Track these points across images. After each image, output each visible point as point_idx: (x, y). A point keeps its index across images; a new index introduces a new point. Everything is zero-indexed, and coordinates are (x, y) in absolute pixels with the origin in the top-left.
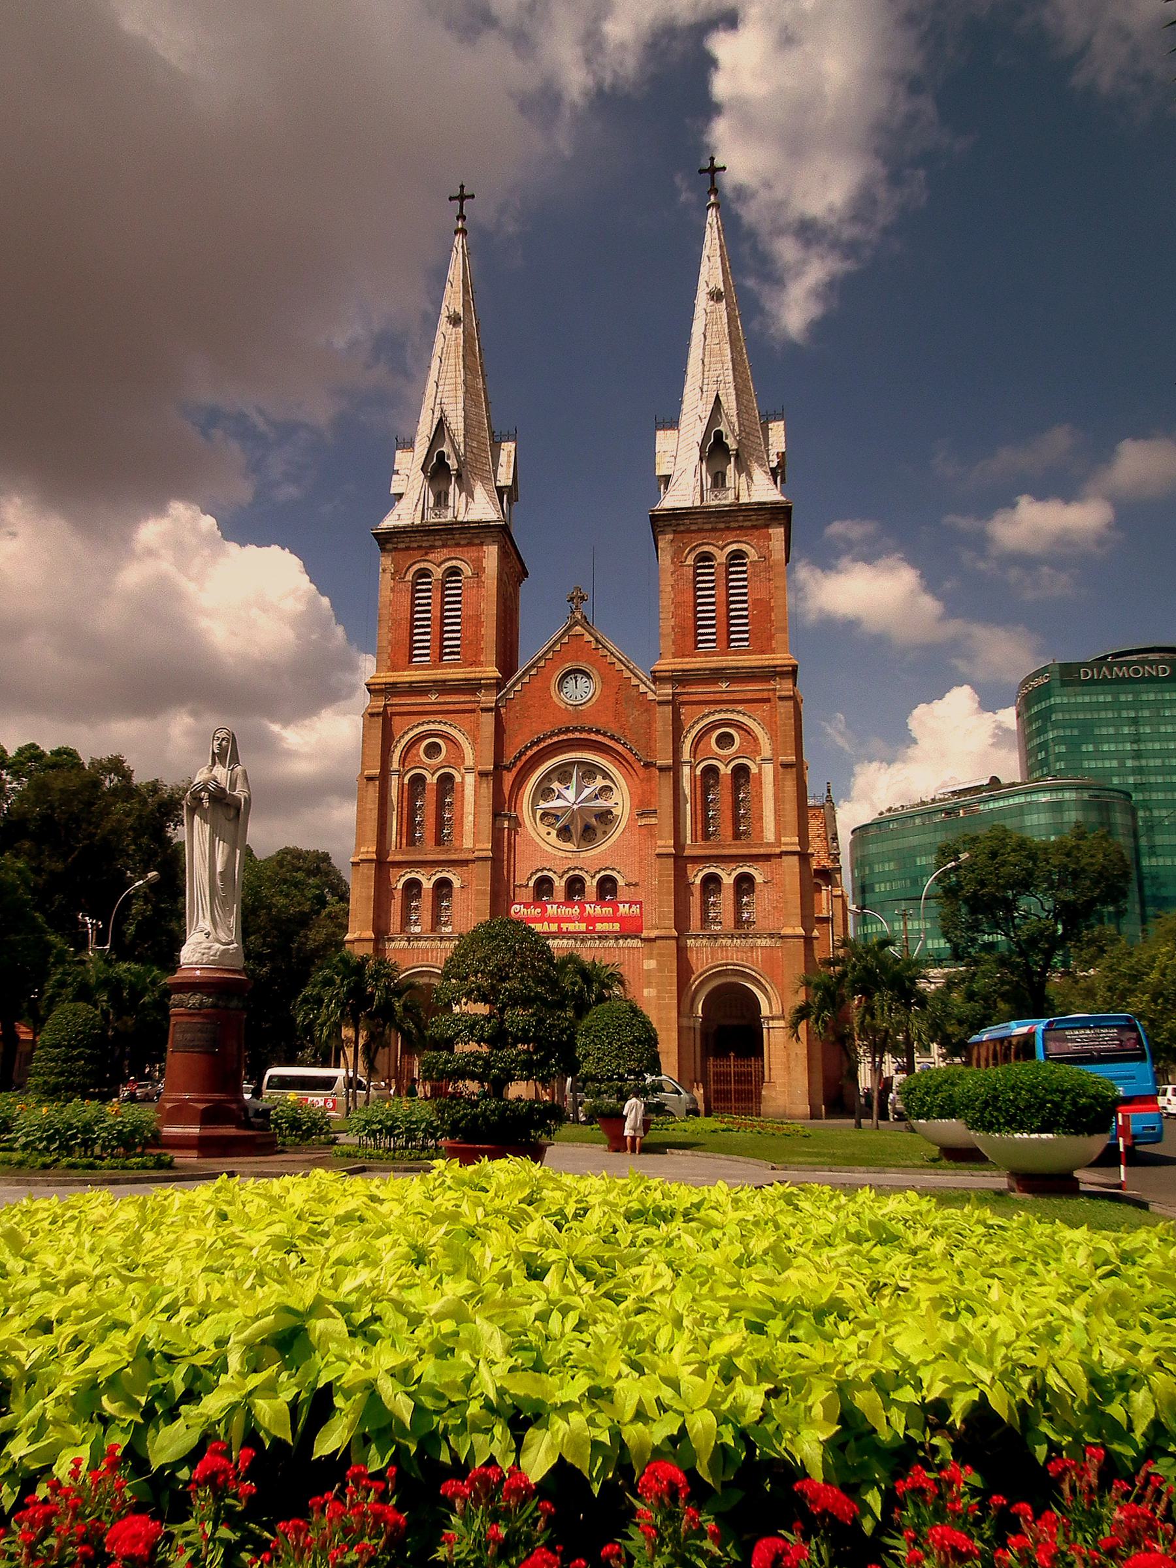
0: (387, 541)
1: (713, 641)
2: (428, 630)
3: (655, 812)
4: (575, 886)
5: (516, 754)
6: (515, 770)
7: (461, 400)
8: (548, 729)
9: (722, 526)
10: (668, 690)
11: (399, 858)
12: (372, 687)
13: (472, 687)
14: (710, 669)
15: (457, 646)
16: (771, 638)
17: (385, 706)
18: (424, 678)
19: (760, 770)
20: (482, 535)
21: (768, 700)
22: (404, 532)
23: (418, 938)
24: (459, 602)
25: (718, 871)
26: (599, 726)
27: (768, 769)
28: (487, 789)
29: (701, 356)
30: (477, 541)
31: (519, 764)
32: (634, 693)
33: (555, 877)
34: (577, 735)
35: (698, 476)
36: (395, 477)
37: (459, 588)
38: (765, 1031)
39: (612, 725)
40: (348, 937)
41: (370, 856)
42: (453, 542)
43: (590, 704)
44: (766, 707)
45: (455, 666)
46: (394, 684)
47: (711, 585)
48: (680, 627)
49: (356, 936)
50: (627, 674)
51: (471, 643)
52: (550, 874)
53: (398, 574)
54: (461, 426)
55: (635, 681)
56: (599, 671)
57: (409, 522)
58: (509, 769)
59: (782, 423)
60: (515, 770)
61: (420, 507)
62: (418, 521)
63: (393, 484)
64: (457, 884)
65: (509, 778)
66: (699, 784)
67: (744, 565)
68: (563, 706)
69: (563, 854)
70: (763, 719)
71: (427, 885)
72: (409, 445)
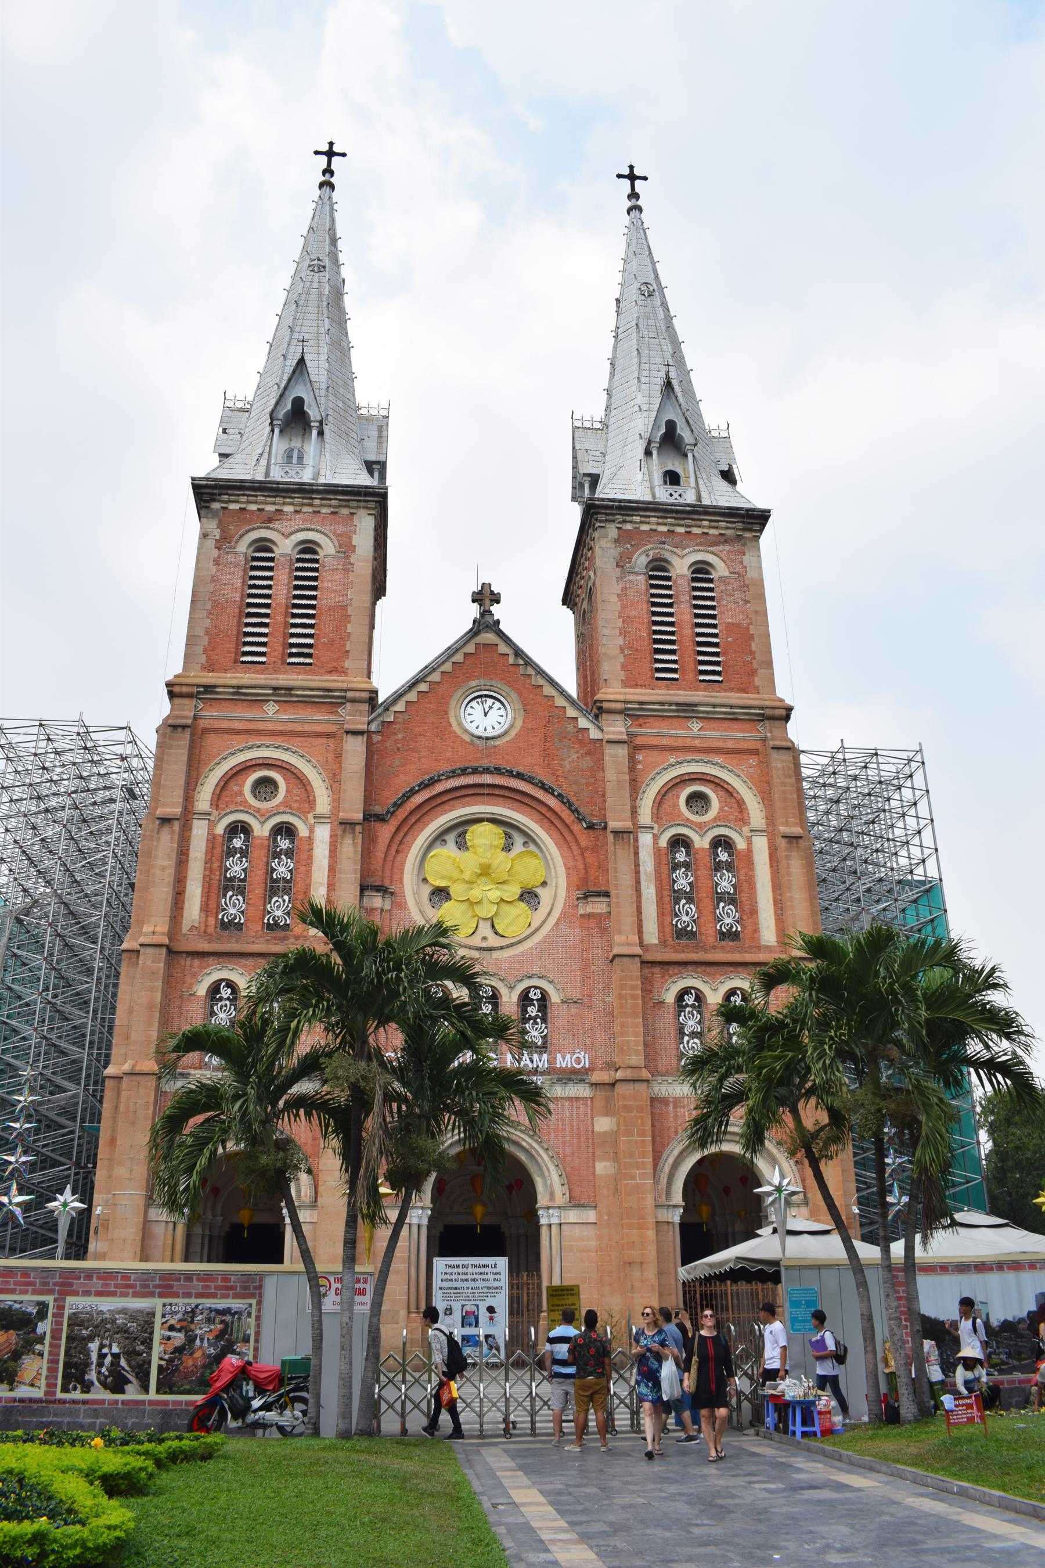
2: (266, 620)
3: (607, 894)
6: (394, 823)
7: (324, 350)
8: (444, 767)
9: (681, 530)
10: (616, 728)
11: (204, 946)
12: (177, 689)
14: (677, 704)
15: (310, 646)
16: (753, 673)
17: (195, 718)
18: (262, 682)
19: (750, 844)
20: (352, 504)
21: (755, 752)
22: (240, 488)
24: (314, 588)
26: (521, 769)
27: (761, 845)
28: (350, 848)
29: (635, 347)
30: (345, 511)
31: (402, 813)
32: (570, 728)
34: (486, 779)
35: (645, 470)
37: (316, 570)
39: (537, 769)
40: (110, 1071)
41: (156, 940)
42: (310, 509)
43: (507, 738)
44: (753, 761)
45: (305, 673)
46: (209, 689)
48: (630, 648)
49: (126, 1067)
50: (560, 702)
51: (331, 642)
54: (323, 378)
55: (571, 712)
56: (520, 693)
57: (248, 477)
58: (381, 819)
60: (394, 823)
61: (264, 462)
62: (260, 477)
65: (385, 832)
66: (664, 858)
67: (711, 581)
68: (467, 738)
70: (750, 777)
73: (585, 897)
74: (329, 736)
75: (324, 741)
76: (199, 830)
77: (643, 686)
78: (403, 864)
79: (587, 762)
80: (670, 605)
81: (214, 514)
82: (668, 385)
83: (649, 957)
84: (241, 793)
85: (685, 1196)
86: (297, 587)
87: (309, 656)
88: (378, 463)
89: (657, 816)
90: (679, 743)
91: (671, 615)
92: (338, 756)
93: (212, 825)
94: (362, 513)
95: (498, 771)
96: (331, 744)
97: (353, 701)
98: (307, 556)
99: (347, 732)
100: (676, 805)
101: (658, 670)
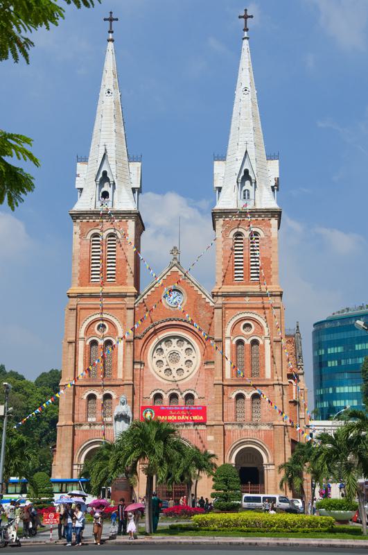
0: (78, 218)
1: (242, 277)
3: (213, 362)
4: (174, 396)
5: (144, 331)
6: (144, 339)
10: (220, 301)
12: (70, 295)
13: (122, 296)
15: (114, 274)
16: (271, 276)
17: (77, 304)
23: (95, 424)
24: (115, 251)
25: (243, 392)
27: (268, 341)
28: (129, 349)
32: (203, 302)
33: (163, 394)
34: (174, 322)
36: (77, 178)
38: (265, 471)
40: (58, 424)
45: (113, 285)
47: (242, 248)
49: (63, 423)
50: (200, 292)
52: (161, 392)
53: (82, 235)
55: (204, 296)
56: (186, 290)
59: (278, 161)
61: (94, 200)
62: (93, 209)
63: (77, 182)
64: (114, 397)
65: (141, 342)
68: (168, 307)
69: (167, 382)
71: (100, 397)
72: (85, 160)
73: (207, 363)
74: (122, 309)
75: (120, 310)
76: (81, 344)
77: (231, 284)
78: (147, 353)
79: (209, 315)
80: (242, 250)
81: (78, 223)
82: (246, 152)
83: (225, 383)
84: (94, 330)
85: (236, 462)
86: (109, 251)
87: (114, 278)
88: (137, 188)
89: (232, 332)
90: (241, 306)
91: (242, 254)
92: (125, 316)
93: (85, 342)
94: (130, 221)
95: (178, 320)
96: (122, 312)
97: (129, 296)
98: (112, 238)
99: (128, 309)
100: (240, 329)
101: (236, 277)
